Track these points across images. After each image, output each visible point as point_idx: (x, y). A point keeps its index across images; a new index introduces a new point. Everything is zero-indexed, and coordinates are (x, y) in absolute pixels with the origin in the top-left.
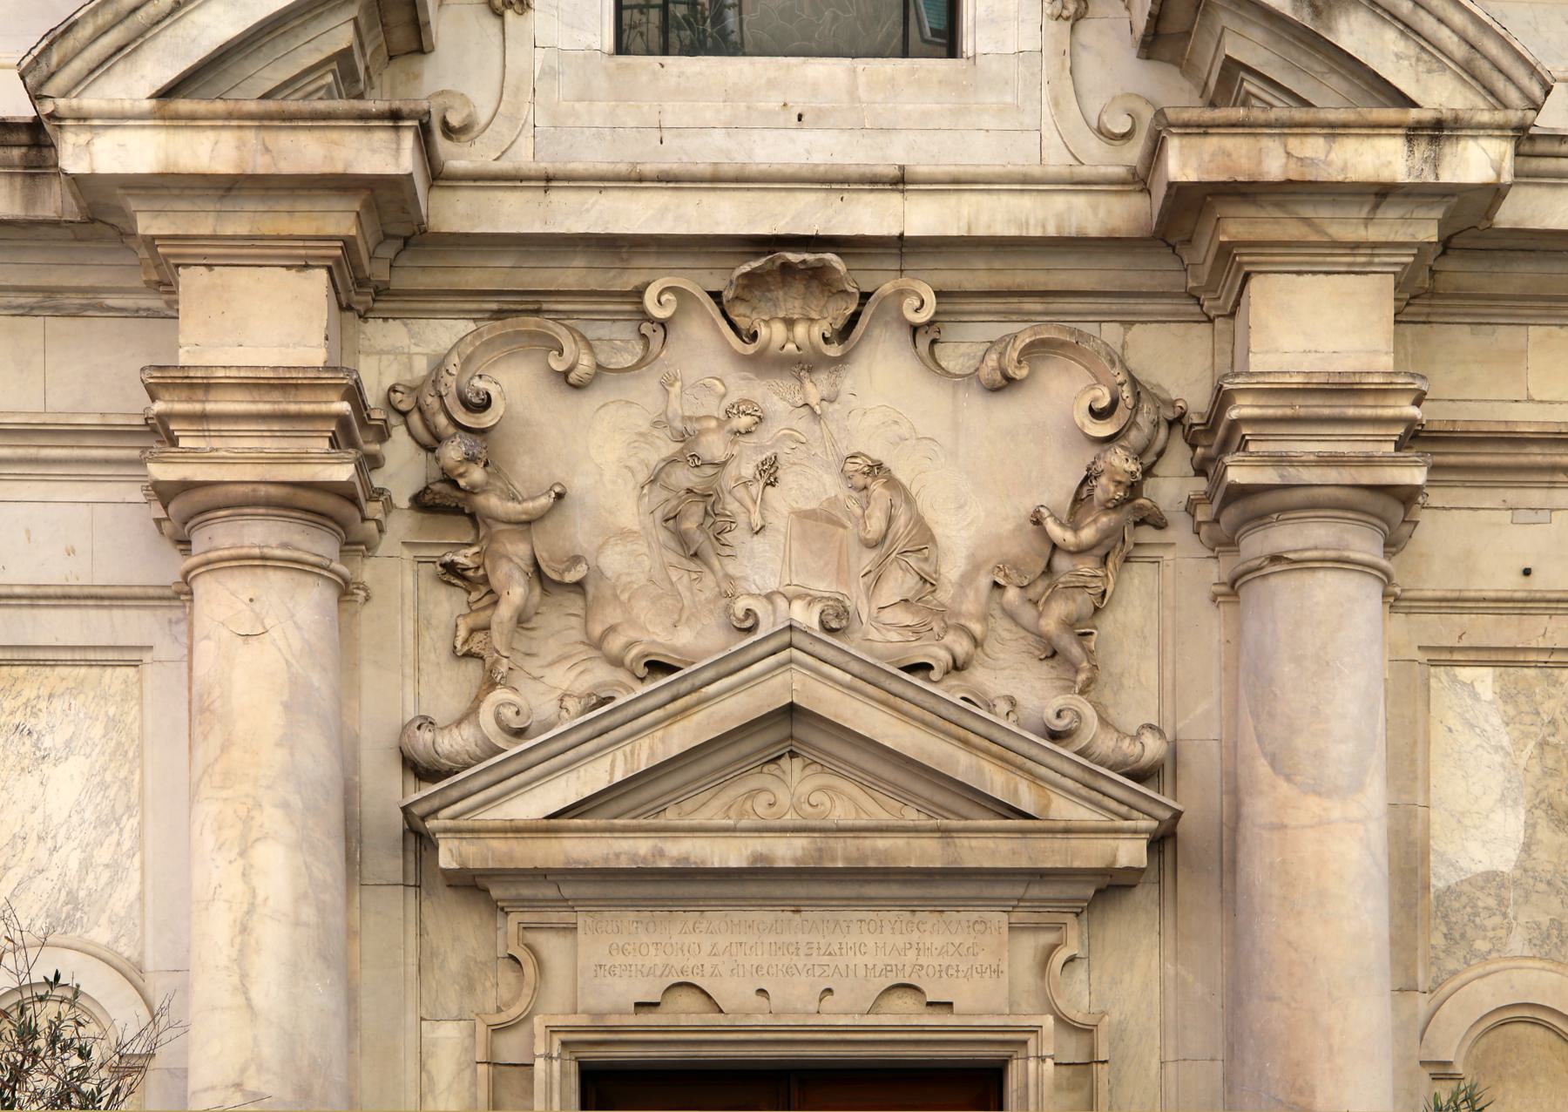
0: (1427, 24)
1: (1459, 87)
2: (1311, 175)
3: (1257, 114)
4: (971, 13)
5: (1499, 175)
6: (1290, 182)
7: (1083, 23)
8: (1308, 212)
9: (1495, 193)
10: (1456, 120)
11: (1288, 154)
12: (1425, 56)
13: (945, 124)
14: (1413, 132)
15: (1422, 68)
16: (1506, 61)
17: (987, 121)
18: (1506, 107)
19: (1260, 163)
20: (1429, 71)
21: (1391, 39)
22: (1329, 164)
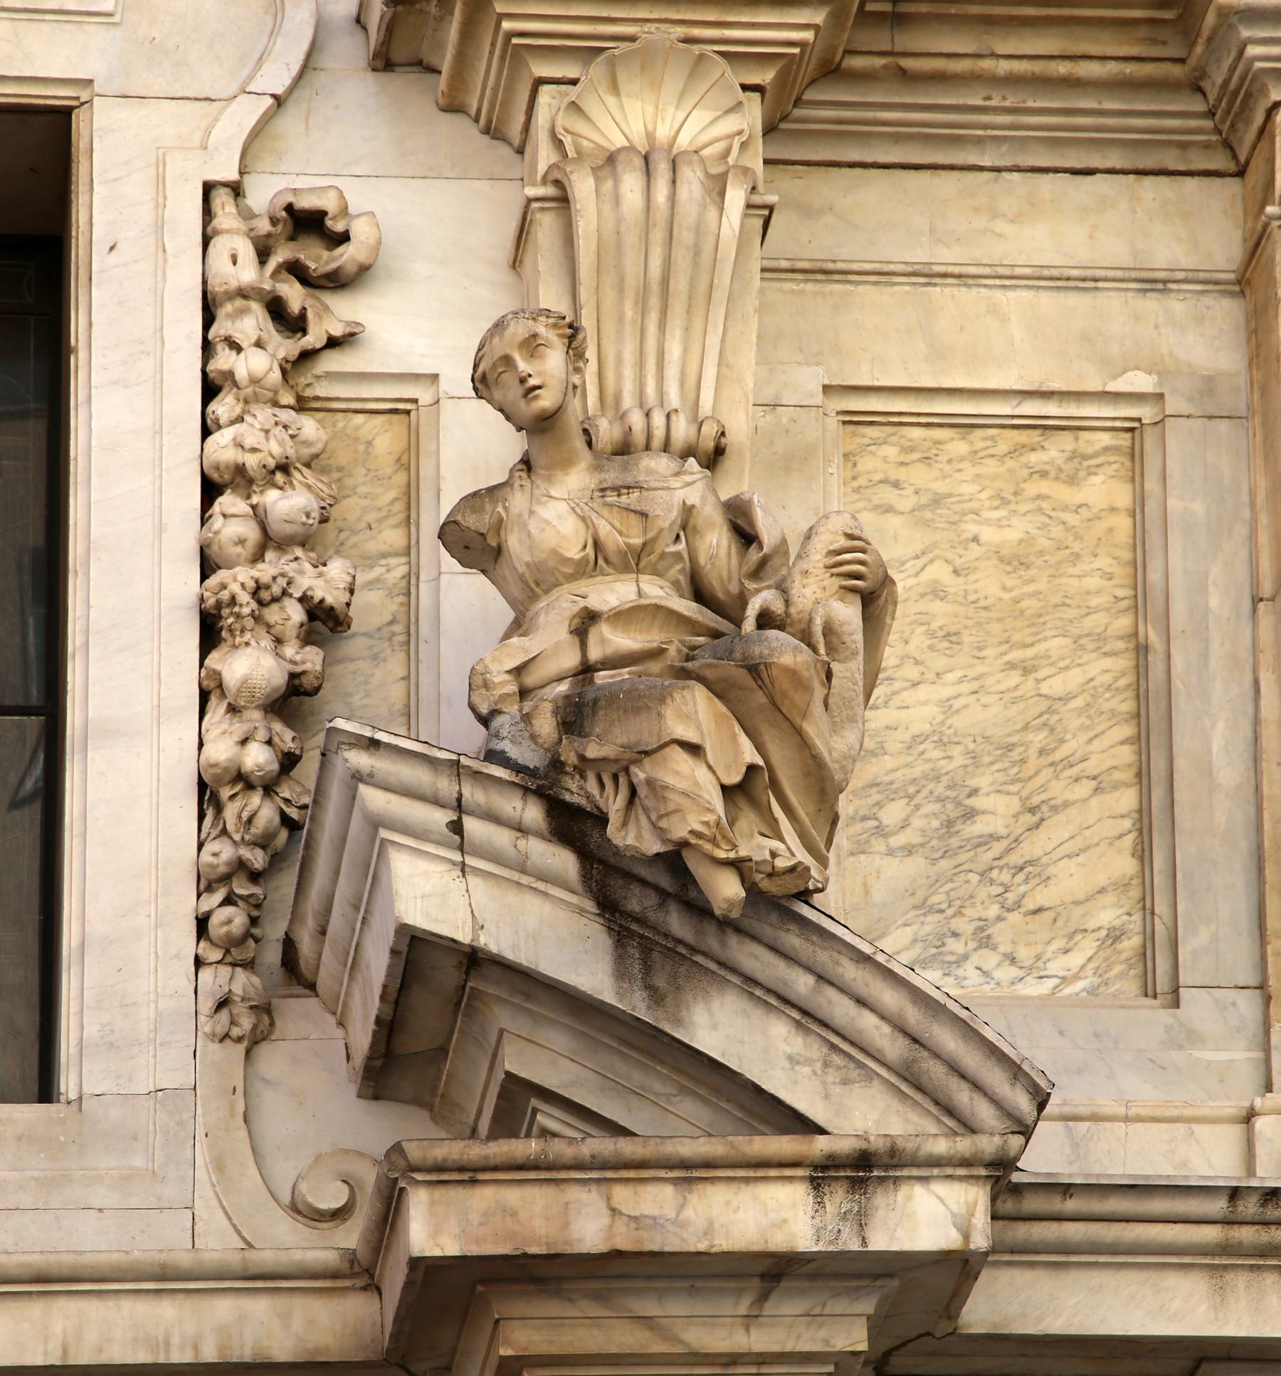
0: (840, 1009)
1: (895, 1104)
2: (653, 1243)
3: (559, 1149)
4: (74, 1035)
5: (966, 1237)
6: (617, 1254)
7: (265, 1049)
8: (648, 1307)
9: (960, 1268)
10: (893, 1152)
11: (614, 1211)
12: (837, 1059)
13: (27, 1201)
14: (822, 1174)
15: (832, 1076)
16: (971, 1059)
17: (101, 1196)
18: (974, 1131)
19: (566, 1225)
20: (845, 1082)
21: (780, 1035)
22: (683, 1225)
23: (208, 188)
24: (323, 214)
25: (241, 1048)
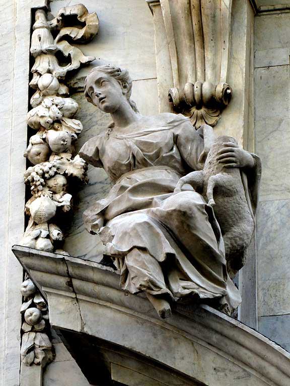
23: (34, 11)
24: (75, 16)
25: (39, 368)
